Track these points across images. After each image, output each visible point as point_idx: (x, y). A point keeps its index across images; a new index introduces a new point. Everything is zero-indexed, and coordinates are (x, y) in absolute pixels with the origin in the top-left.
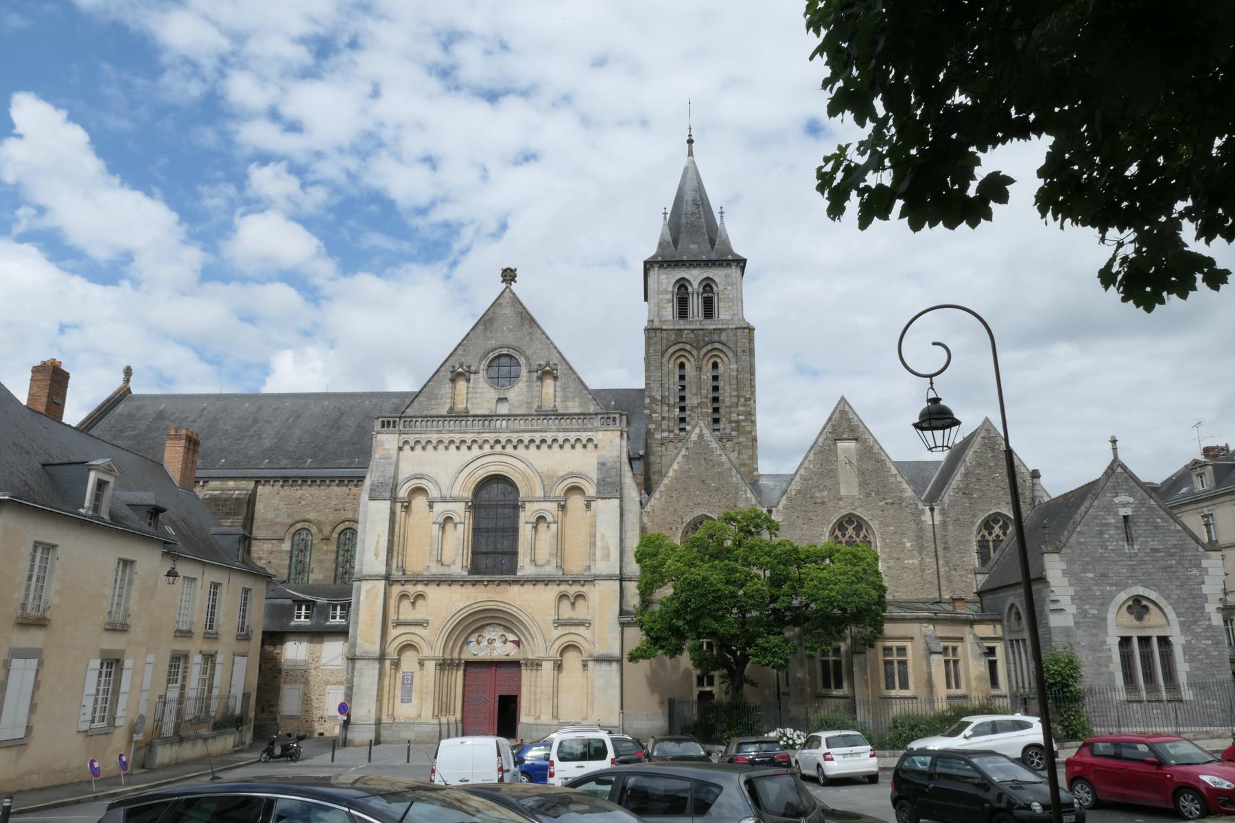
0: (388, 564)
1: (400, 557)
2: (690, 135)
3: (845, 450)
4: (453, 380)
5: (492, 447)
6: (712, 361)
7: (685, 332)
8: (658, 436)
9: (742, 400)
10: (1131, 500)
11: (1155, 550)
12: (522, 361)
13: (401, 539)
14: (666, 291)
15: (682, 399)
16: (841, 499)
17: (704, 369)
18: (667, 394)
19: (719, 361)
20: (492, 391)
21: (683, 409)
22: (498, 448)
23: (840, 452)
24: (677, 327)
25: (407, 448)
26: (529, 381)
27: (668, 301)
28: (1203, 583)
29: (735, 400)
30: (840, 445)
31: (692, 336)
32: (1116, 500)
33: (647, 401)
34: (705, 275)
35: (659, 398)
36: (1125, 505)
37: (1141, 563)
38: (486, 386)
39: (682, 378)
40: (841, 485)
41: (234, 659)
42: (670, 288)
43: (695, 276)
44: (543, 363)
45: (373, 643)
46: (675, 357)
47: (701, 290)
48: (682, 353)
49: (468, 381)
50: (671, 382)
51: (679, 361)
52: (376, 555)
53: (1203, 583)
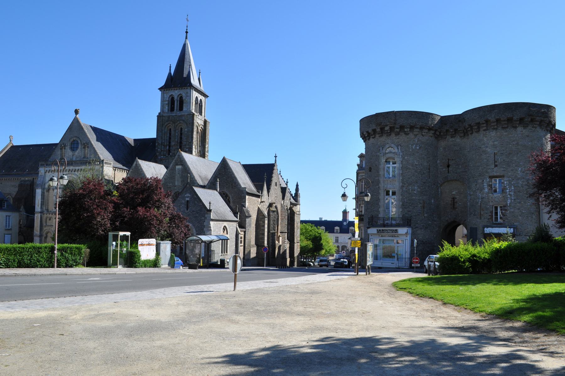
0: (41, 208)
1: (46, 206)
2: (187, 30)
3: (178, 169)
4: (61, 149)
5: (69, 172)
6: (180, 128)
7: (171, 117)
8: (159, 158)
9: (188, 143)
10: (190, 195)
11: (193, 211)
12: (80, 142)
13: (47, 201)
14: (166, 101)
15: (170, 143)
16: (175, 186)
17: (177, 131)
18: (163, 141)
19: (182, 127)
20: (71, 152)
21: (170, 146)
22: (70, 172)
23: (177, 170)
24: (168, 115)
25: (47, 172)
26: (81, 149)
27: (166, 104)
28: (205, 222)
29: (185, 143)
30: (178, 167)
31: (173, 118)
32: (186, 195)
33: (157, 144)
34: (179, 93)
35: (160, 143)
36: (188, 197)
37: (189, 215)
38: (70, 151)
39: (170, 134)
40: (176, 182)
41: (5, 236)
42: (167, 99)
43: (176, 93)
44: (85, 142)
45: (38, 232)
46: (167, 127)
47: (179, 99)
48: (170, 125)
49: (65, 149)
50: (166, 137)
51: (169, 128)
52: (38, 206)
53: (205, 222)
